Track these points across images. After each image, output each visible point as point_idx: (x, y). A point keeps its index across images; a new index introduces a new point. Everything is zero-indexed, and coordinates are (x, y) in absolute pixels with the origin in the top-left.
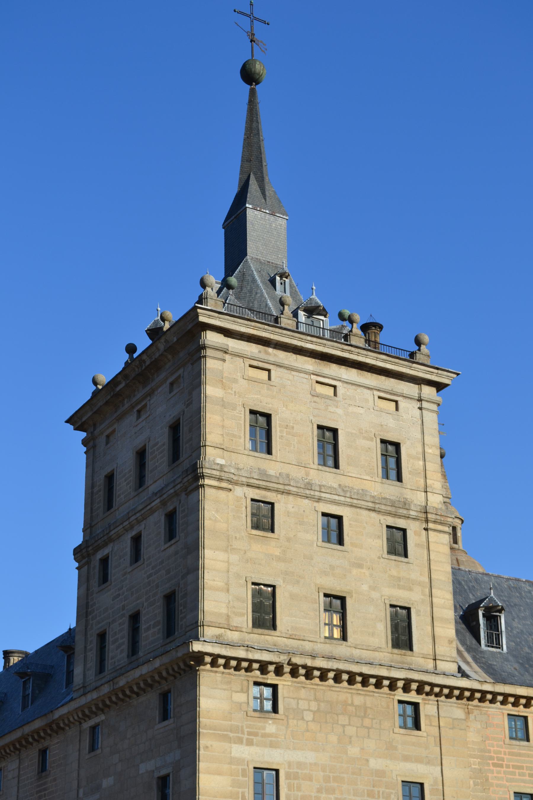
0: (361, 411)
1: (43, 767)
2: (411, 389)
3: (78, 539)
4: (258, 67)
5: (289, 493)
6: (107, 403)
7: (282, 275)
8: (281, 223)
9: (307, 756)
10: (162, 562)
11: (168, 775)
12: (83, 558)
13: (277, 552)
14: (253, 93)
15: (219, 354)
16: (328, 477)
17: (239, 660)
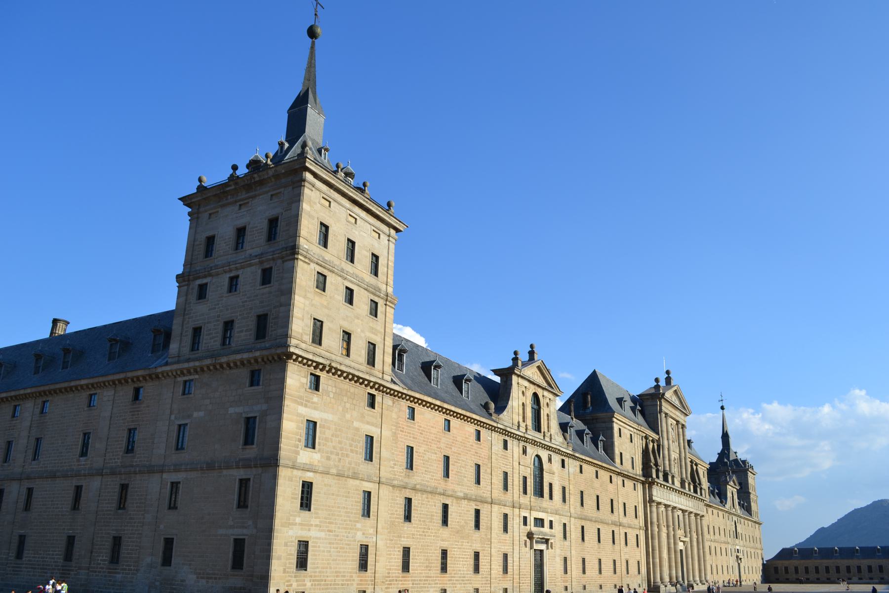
0: (365, 235)
1: (136, 397)
2: (385, 228)
3: (180, 271)
4: (319, 30)
5: (333, 272)
6: (215, 195)
7: (326, 150)
8: (322, 119)
9: (329, 416)
10: (257, 296)
11: (255, 417)
12: (184, 281)
13: (325, 303)
14: (313, 43)
15: (310, 187)
16: (348, 266)
17: (308, 360)
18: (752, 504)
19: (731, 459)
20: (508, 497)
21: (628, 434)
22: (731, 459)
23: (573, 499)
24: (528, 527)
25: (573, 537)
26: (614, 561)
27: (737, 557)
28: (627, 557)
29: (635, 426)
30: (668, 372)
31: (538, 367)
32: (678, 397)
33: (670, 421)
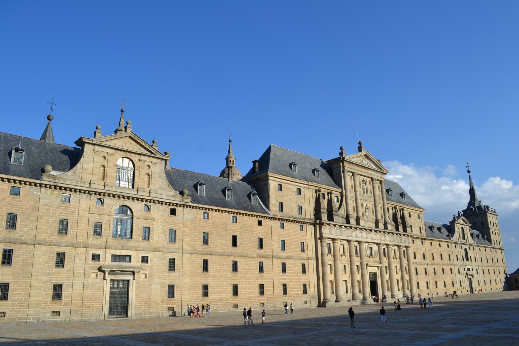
18: (492, 236)
19: (476, 206)
20: (69, 238)
21: (295, 189)
22: (477, 205)
23: (190, 240)
24: (101, 263)
25: (187, 267)
26: (262, 287)
27: (467, 274)
28: (284, 282)
29: (303, 182)
30: (360, 143)
31: (130, 137)
32: (371, 160)
33: (362, 178)
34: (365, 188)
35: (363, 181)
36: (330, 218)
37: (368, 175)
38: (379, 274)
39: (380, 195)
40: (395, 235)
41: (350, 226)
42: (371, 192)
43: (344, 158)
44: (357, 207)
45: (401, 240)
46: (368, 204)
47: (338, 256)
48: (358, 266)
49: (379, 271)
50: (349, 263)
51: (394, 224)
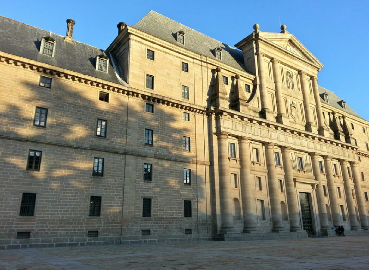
28: (147, 194)
29: (192, 54)
34: (290, 80)
35: (288, 72)
36: (235, 104)
37: (294, 66)
38: (315, 195)
39: (311, 94)
40: (334, 146)
41: (267, 122)
42: (299, 88)
43: (257, 35)
44: (278, 101)
45: (344, 153)
46: (294, 102)
47: (248, 163)
48: (281, 181)
49: (314, 191)
50: (266, 175)
51: (333, 133)
